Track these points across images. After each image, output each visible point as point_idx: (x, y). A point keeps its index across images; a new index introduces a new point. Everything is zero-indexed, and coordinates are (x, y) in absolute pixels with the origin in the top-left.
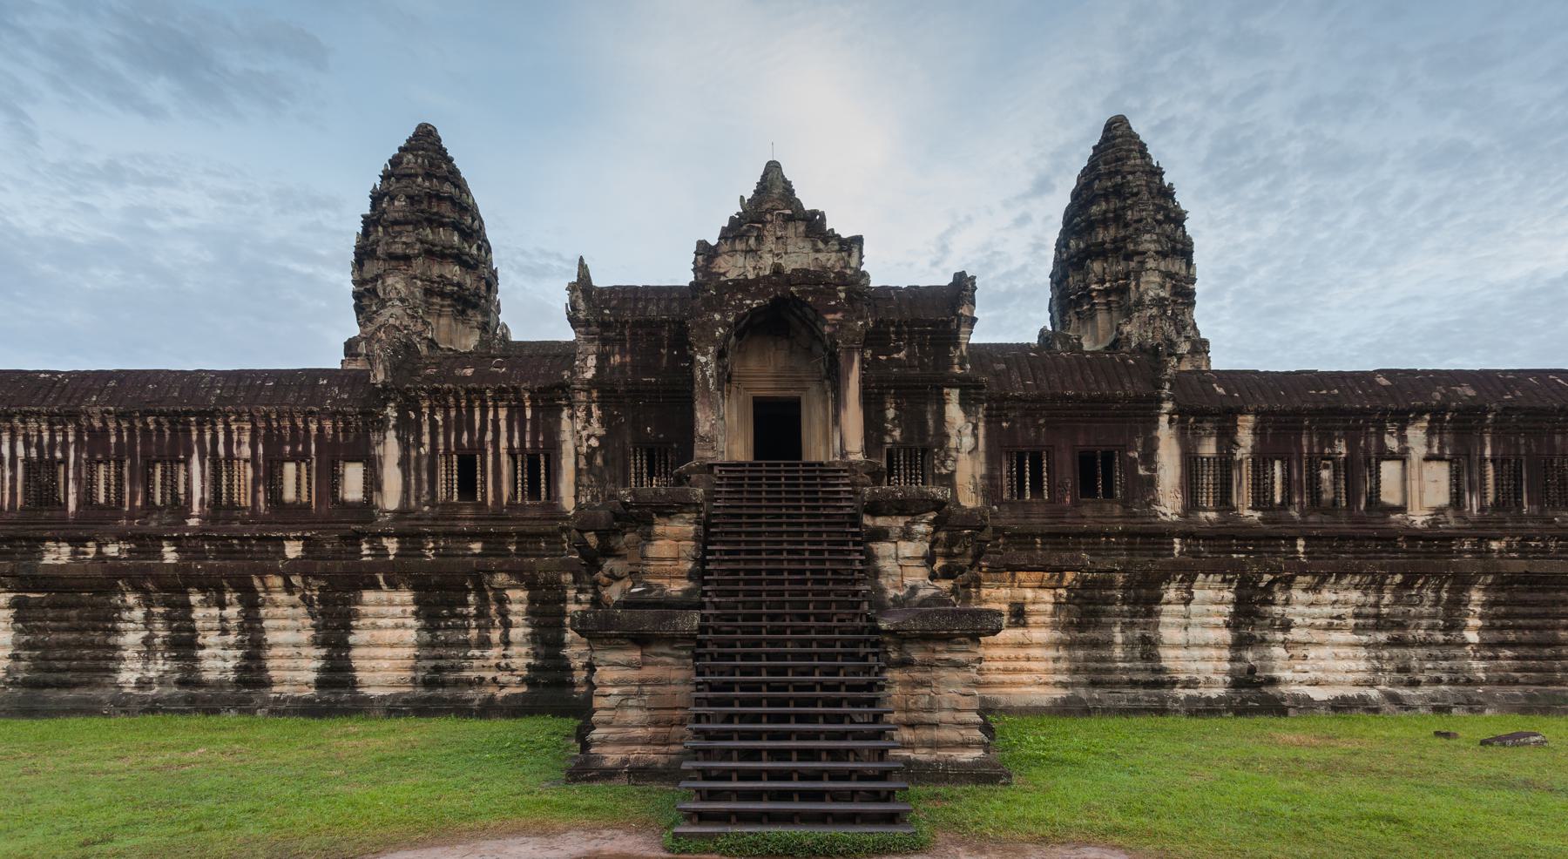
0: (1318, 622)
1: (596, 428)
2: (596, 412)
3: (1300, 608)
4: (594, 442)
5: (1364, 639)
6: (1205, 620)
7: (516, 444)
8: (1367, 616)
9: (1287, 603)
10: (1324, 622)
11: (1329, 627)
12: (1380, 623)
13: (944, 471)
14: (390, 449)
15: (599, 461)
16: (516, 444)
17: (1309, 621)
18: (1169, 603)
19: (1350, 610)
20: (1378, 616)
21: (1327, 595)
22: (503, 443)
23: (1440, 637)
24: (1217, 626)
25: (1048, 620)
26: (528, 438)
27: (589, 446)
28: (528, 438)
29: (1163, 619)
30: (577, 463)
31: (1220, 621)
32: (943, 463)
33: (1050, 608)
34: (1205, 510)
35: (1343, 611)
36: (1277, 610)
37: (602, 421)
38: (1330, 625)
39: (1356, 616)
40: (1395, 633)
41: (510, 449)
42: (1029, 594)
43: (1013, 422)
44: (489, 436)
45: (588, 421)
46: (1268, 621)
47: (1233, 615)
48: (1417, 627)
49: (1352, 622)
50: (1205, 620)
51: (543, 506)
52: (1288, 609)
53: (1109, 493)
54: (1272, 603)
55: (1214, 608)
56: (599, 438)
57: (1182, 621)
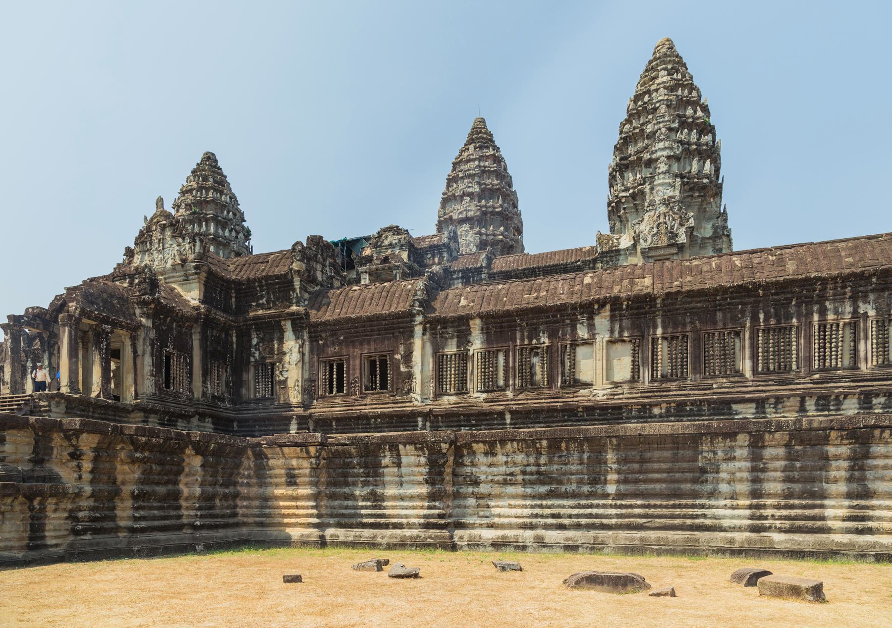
0: (496, 478)
3: (484, 468)
5: (529, 490)
6: (412, 478)
8: (532, 474)
9: (473, 465)
10: (500, 478)
11: (505, 483)
12: (542, 478)
13: (282, 378)
17: (490, 478)
18: (387, 467)
19: (517, 470)
20: (538, 473)
21: (501, 458)
23: (586, 489)
24: (420, 483)
25: (307, 479)
29: (387, 479)
31: (420, 478)
32: (281, 372)
33: (307, 471)
34: (449, 395)
35: (513, 469)
36: (468, 470)
38: (505, 480)
39: (524, 473)
40: (553, 487)
42: (294, 462)
43: (326, 340)
46: (461, 479)
47: (429, 473)
48: (570, 482)
49: (520, 478)
50: (412, 478)
52: (474, 469)
53: (384, 386)
54: (463, 465)
55: (417, 469)
57: (397, 479)
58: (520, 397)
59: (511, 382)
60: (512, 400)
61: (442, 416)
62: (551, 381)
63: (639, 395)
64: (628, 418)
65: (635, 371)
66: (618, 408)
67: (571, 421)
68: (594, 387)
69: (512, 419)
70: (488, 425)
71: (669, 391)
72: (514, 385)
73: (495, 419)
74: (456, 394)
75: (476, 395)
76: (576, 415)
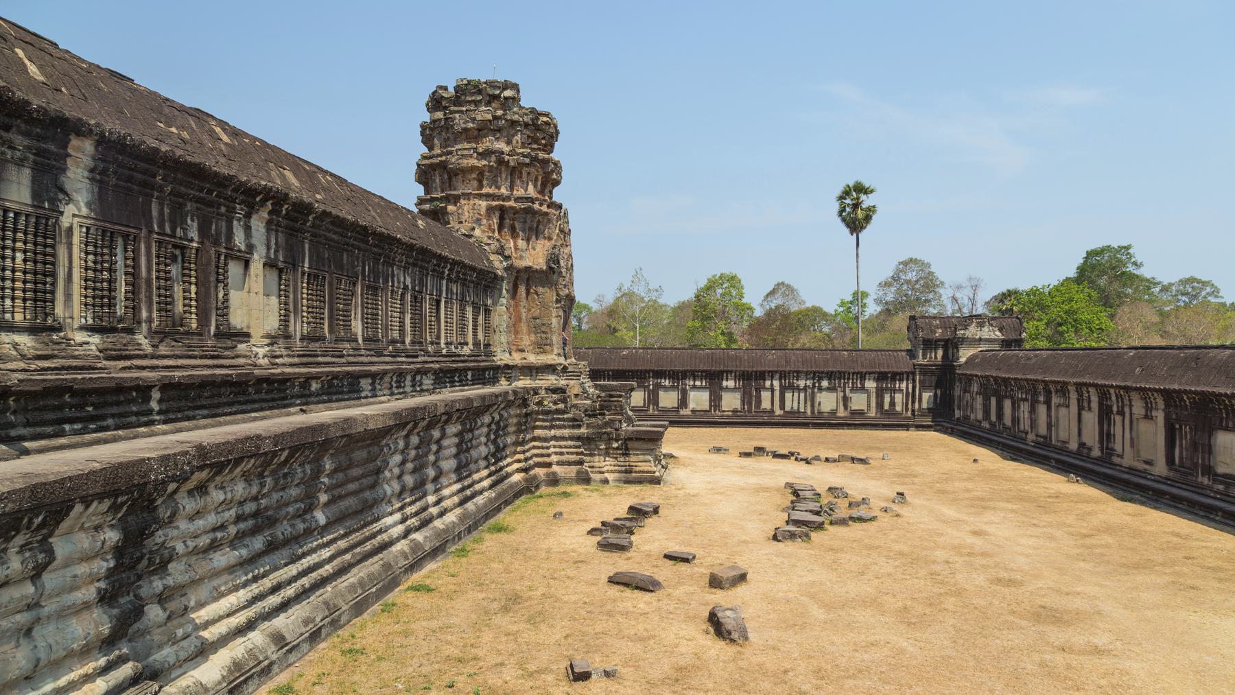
58: (163, 349)
59: (144, 314)
60: (153, 357)
61: (20, 395)
62: (204, 320)
63: (296, 360)
64: (292, 397)
65: (285, 320)
66: (285, 381)
67: (240, 403)
68: (253, 341)
69: (160, 402)
70: (121, 415)
71: (317, 356)
72: (150, 320)
73: (133, 401)
74: (33, 330)
75: (80, 337)
76: (244, 393)
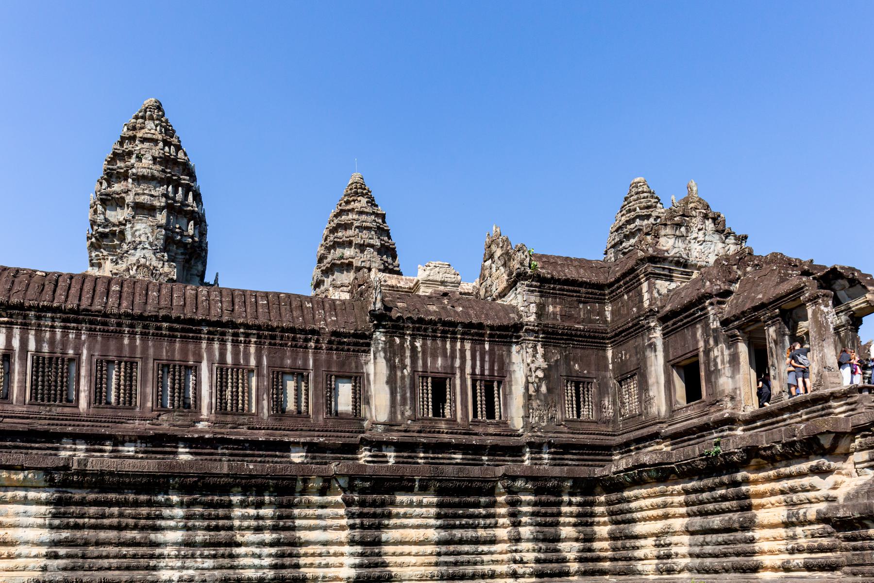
1: (541, 362)
2: (540, 350)
4: (540, 374)
7: (478, 371)
14: (376, 368)
15: (544, 389)
16: (478, 371)
22: (468, 370)
26: (487, 366)
27: (537, 377)
28: (487, 366)
30: (527, 388)
37: (544, 356)
41: (473, 374)
44: (457, 363)
45: (534, 356)
51: (497, 424)
56: (544, 370)
